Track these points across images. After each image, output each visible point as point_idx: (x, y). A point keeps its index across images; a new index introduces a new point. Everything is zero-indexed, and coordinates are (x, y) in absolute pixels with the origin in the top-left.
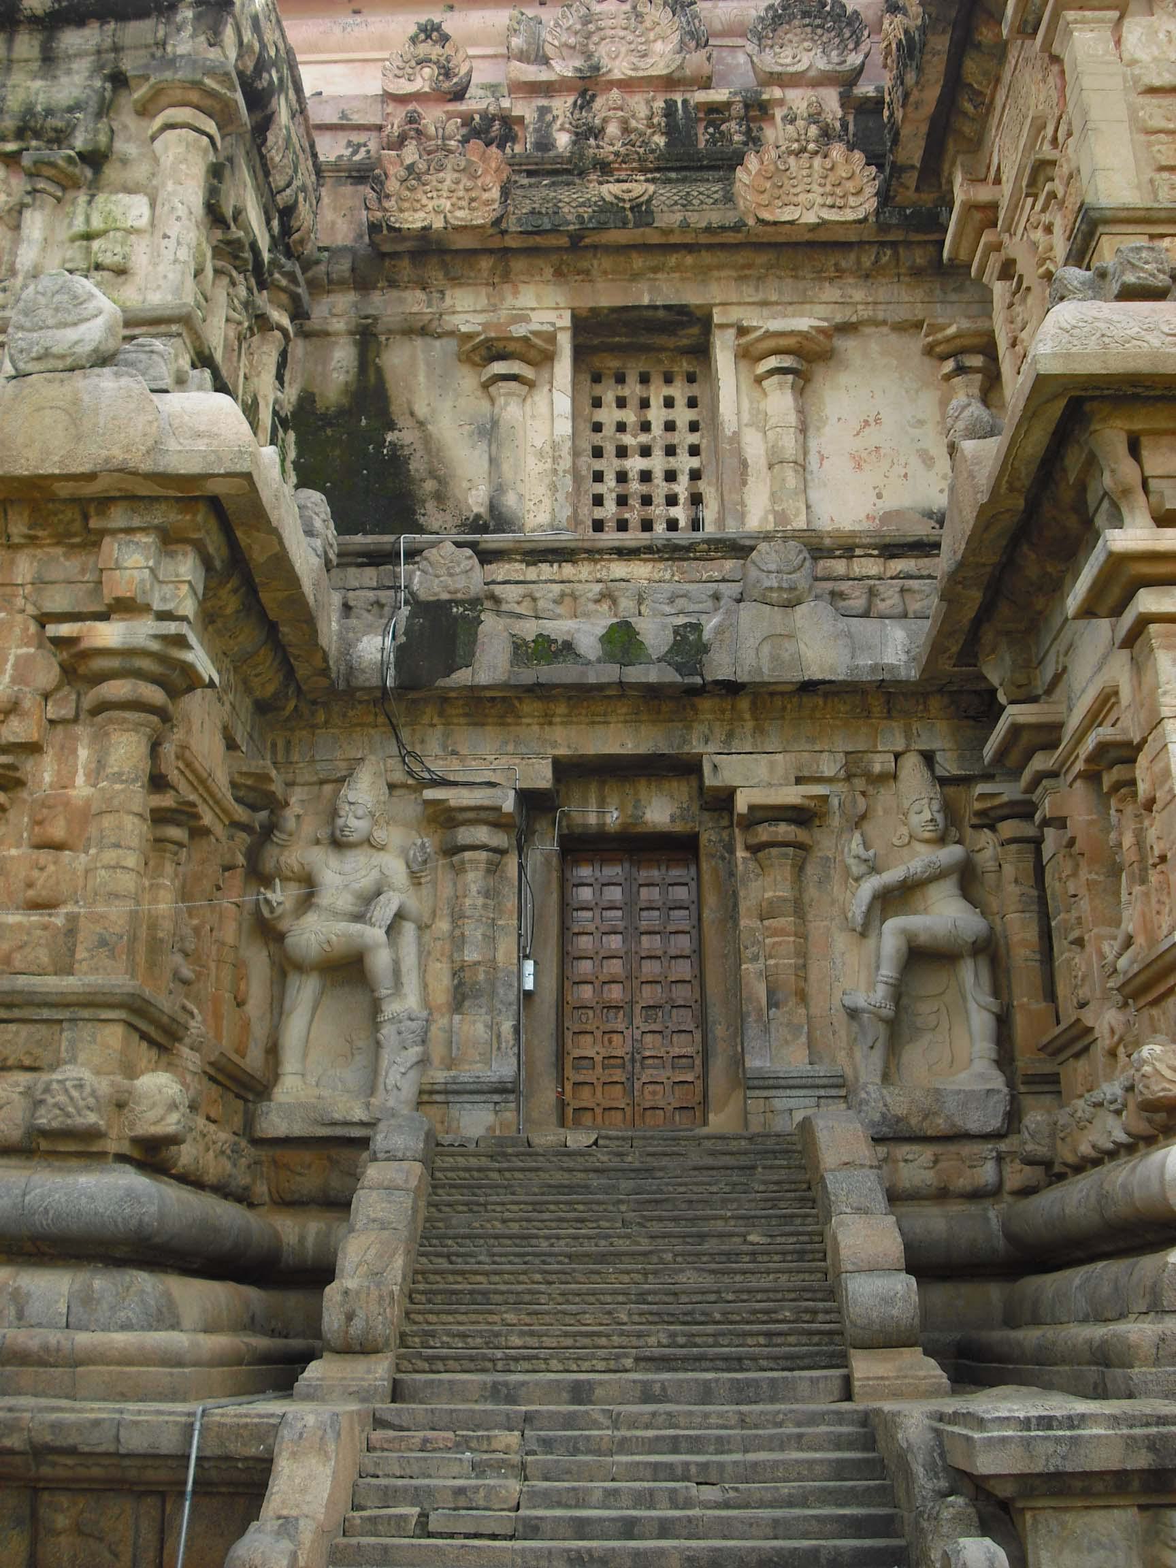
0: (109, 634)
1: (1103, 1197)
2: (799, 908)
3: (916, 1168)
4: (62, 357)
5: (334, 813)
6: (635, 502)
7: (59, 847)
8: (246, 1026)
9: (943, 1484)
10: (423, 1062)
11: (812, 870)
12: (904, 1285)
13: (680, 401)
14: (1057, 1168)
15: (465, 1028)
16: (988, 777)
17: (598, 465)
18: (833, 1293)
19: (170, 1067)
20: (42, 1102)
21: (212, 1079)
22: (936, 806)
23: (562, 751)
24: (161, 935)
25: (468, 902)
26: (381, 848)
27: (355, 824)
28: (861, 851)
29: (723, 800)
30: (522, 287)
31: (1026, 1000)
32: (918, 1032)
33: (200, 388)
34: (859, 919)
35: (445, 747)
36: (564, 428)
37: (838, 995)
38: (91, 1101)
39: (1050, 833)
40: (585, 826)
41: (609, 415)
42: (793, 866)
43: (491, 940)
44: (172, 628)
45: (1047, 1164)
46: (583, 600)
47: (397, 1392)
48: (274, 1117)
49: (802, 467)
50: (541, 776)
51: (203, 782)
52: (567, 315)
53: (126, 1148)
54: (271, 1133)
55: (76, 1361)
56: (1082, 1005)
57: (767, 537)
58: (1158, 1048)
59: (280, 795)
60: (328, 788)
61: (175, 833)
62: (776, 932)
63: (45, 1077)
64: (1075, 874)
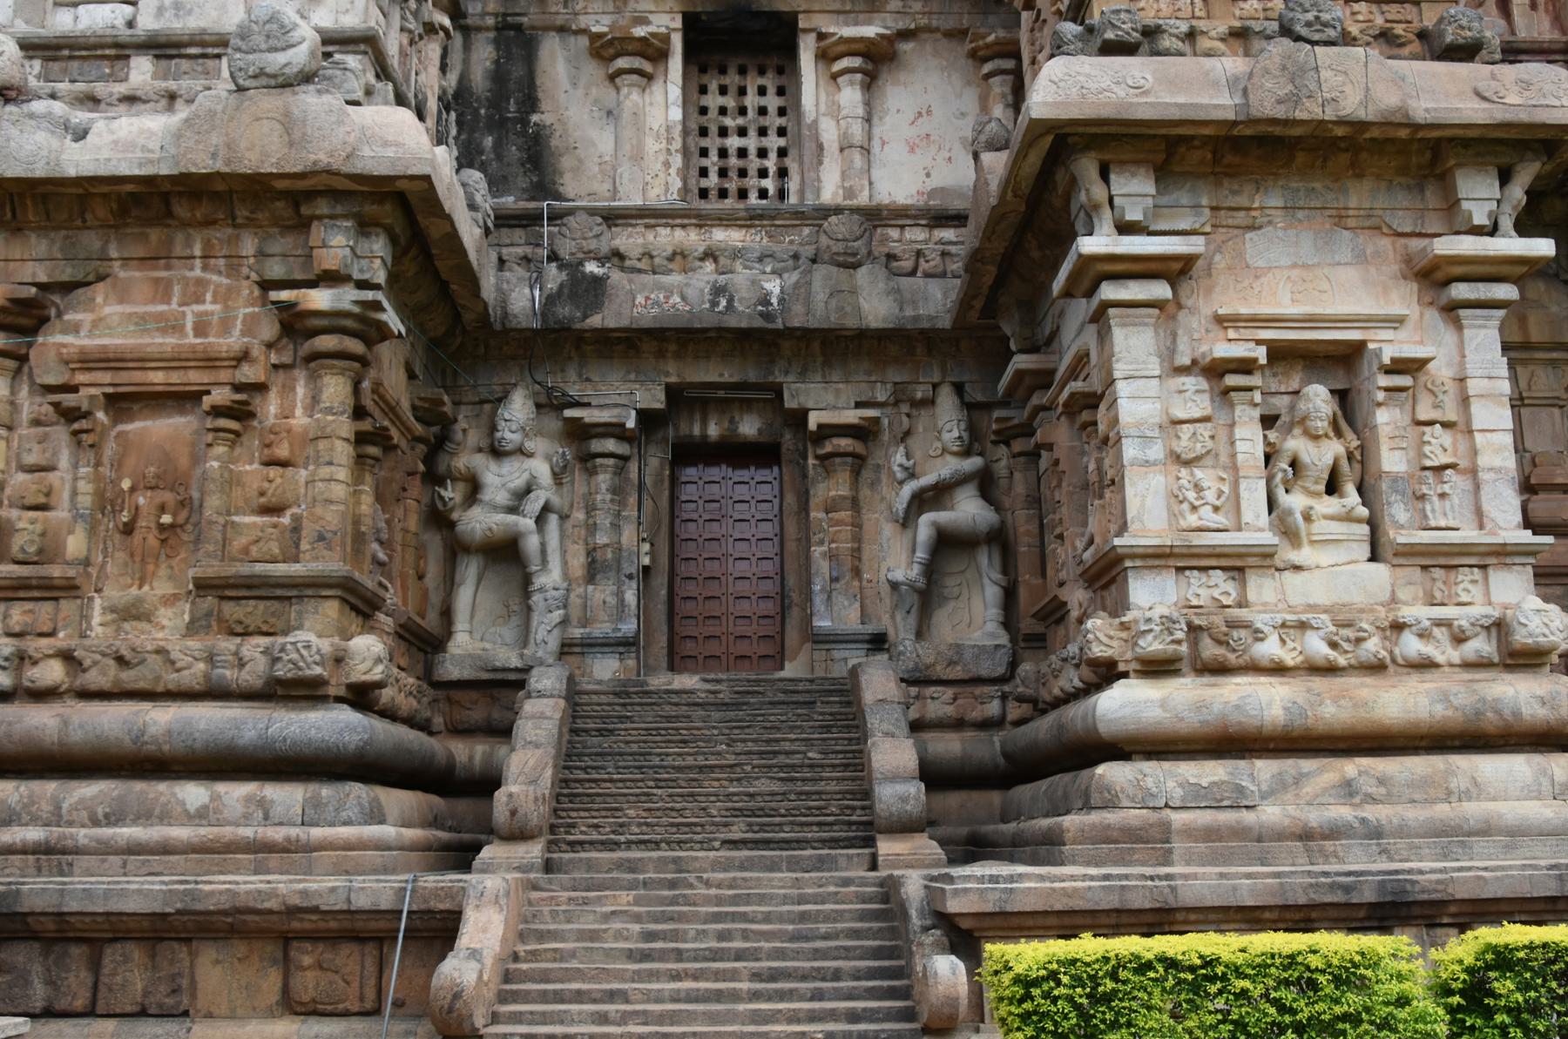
0: (320, 299)
1: (1061, 727)
2: (855, 504)
3: (939, 704)
4: (274, 76)
5: (493, 428)
6: (733, 174)
7: (284, 464)
8: (425, 594)
9: (928, 922)
10: (564, 622)
11: (867, 474)
12: (916, 789)
13: (771, 90)
14: (1041, 706)
16: (1004, 403)
17: (704, 143)
18: (867, 794)
19: (371, 630)
20: (279, 659)
21: (401, 637)
22: (963, 426)
23: (673, 379)
24: (363, 529)
25: (599, 497)
26: (530, 455)
27: (509, 436)
28: (904, 461)
31: (1026, 577)
32: (945, 599)
33: (386, 103)
34: (901, 514)
35: (580, 376)
36: (676, 114)
38: (317, 658)
39: (1043, 453)
40: (691, 436)
41: (713, 100)
43: (616, 527)
44: (369, 295)
45: (1033, 701)
47: (548, 867)
48: (448, 665)
49: (866, 150)
51: (392, 409)
52: (679, 18)
53: (342, 692)
54: (446, 677)
55: (310, 848)
56: (1061, 584)
57: (838, 210)
58: (1099, 622)
59: (450, 413)
60: (487, 407)
61: (373, 450)
62: (838, 523)
63: (280, 640)
64: (1059, 485)
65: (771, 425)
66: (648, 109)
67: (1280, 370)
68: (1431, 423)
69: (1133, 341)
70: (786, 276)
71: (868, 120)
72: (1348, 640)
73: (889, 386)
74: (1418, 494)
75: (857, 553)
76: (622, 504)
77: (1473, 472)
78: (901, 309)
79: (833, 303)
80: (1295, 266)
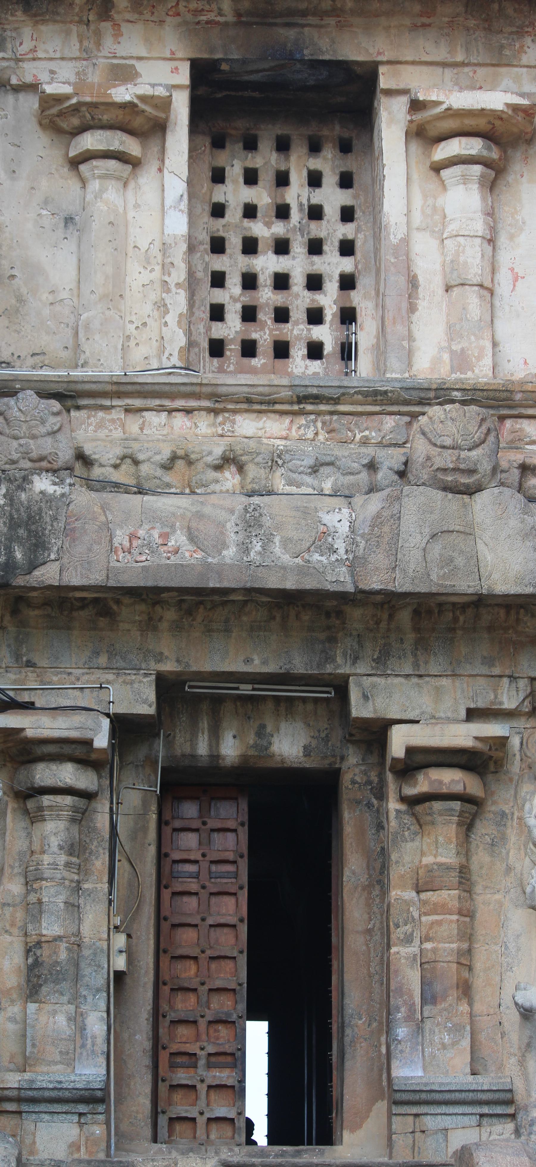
2: (464, 878)
6: (266, 316)
11: (484, 829)
13: (330, 180)
15: (43, 1019)
17: (219, 263)
23: (169, 666)
25: (47, 859)
29: (374, 735)
30: (125, 28)
35: (18, 657)
36: (178, 224)
37: (507, 1000)
40: (194, 756)
41: (235, 194)
42: (459, 824)
43: (73, 908)
46: (200, 466)
49: (488, 290)
50: (138, 698)
52: (185, 70)
57: (439, 394)
65: (326, 740)
66: (131, 214)
70: (358, 500)
71: (491, 241)
73: (522, 684)
75: (465, 959)
76: (83, 869)
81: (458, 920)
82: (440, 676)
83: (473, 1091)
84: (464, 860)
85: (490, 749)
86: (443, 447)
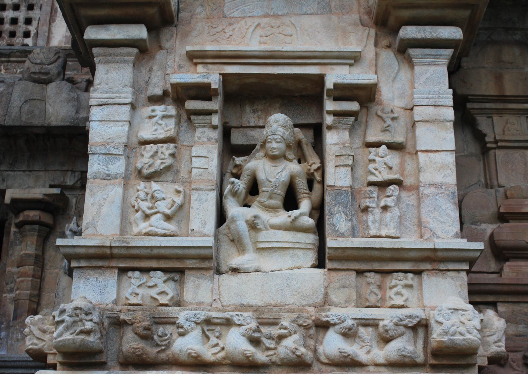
42: (38, 236)
67: (260, 107)
68: (378, 145)
69: (112, 75)
72: (270, 338)
74: (362, 206)
77: (416, 188)
78: (77, 112)
79: (26, 107)
80: (266, 16)
81: (32, 280)
82: (39, 171)
83: (25, 361)
84: (40, 253)
85: (54, 200)
86: (36, 64)
